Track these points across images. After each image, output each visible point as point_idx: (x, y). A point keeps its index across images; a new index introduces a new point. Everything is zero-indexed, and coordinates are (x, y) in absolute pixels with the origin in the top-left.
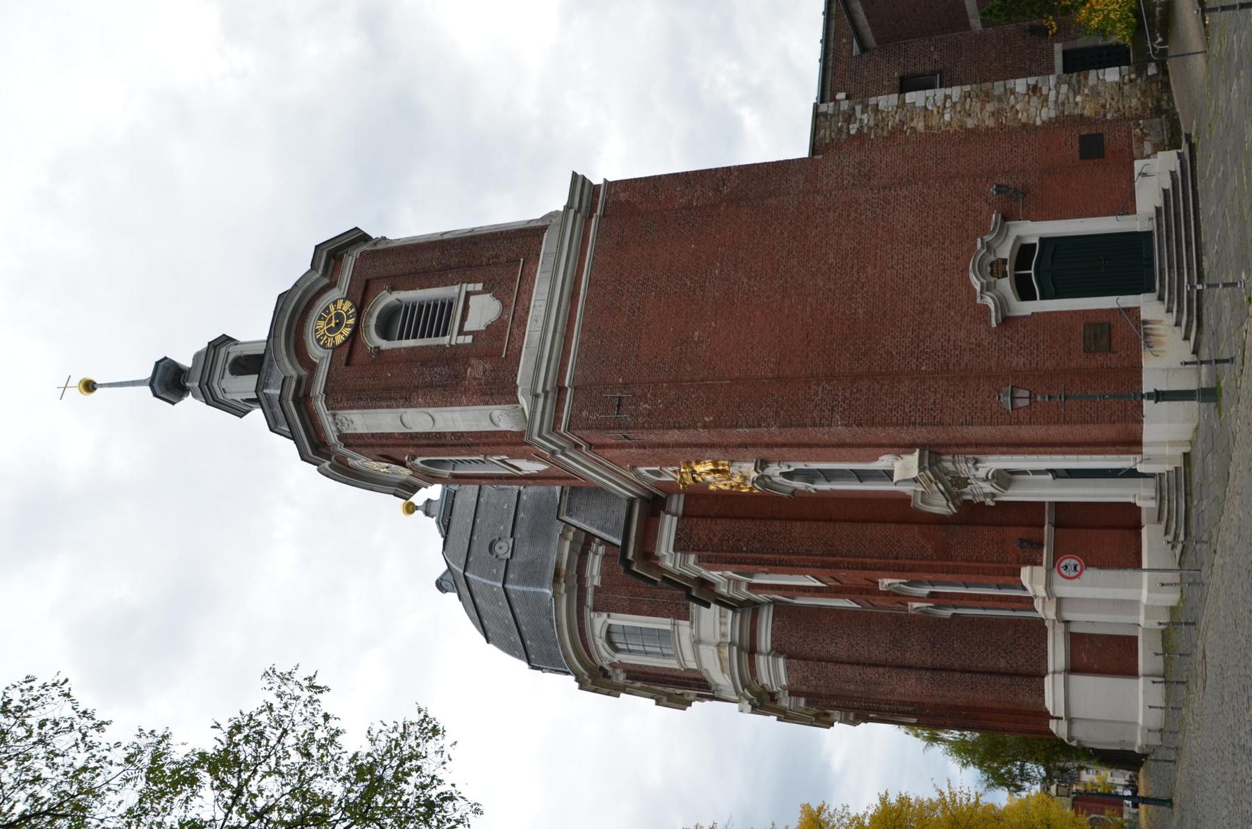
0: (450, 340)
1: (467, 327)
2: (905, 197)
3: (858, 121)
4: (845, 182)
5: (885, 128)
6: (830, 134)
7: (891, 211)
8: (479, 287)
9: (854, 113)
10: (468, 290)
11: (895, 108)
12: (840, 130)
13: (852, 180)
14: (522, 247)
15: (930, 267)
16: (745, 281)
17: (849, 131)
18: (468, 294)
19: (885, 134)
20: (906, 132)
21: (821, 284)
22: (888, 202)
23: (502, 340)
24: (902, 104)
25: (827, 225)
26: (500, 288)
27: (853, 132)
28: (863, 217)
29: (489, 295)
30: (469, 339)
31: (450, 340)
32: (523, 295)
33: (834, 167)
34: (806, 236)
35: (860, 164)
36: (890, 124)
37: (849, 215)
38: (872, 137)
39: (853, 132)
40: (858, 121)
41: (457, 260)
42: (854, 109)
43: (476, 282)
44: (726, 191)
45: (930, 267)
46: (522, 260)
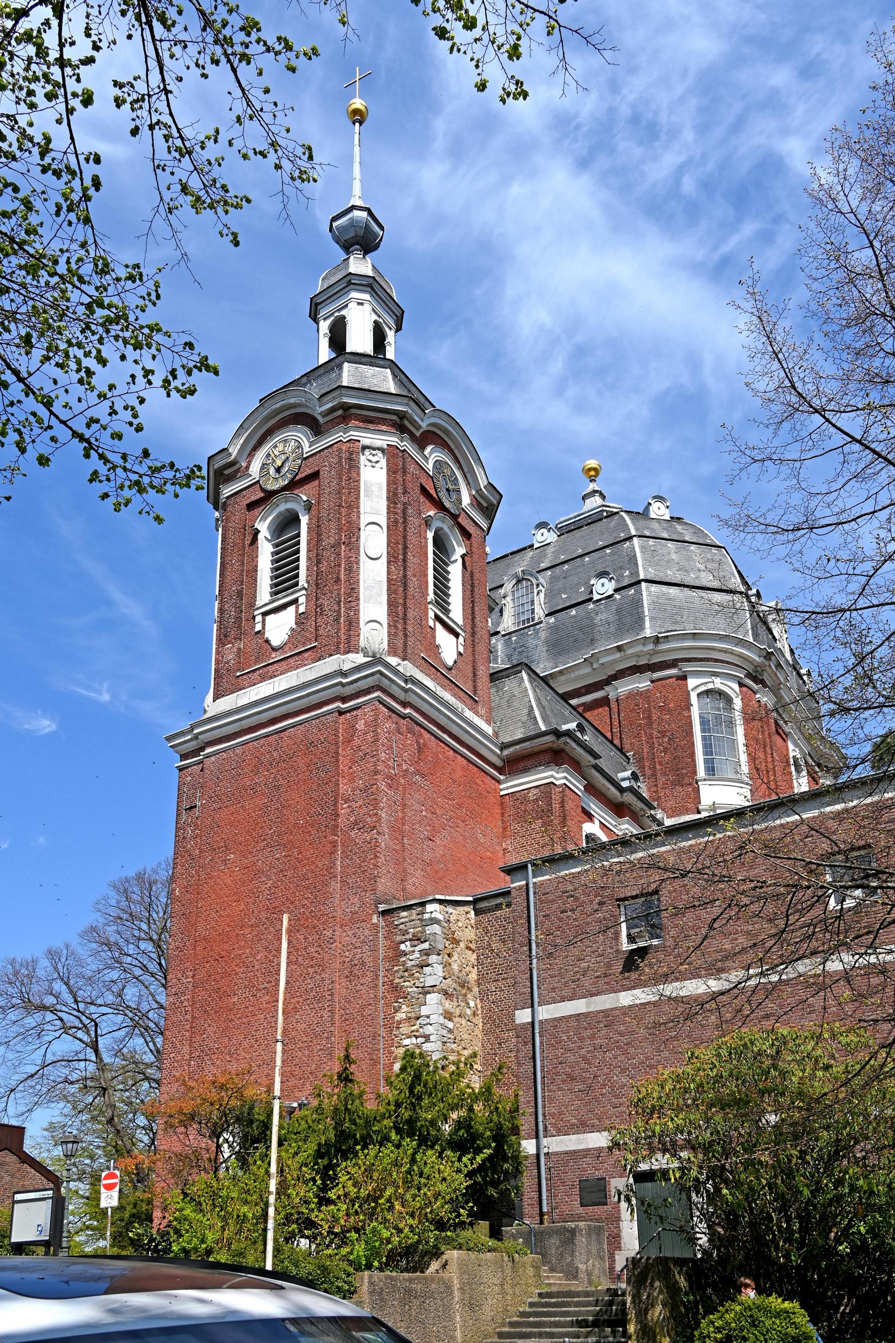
2: (322, 1017)
3: (412, 949)
4: (347, 954)
5: (402, 980)
6: (402, 923)
7: (312, 1006)
9: (422, 942)
11: (422, 985)
12: (406, 932)
13: (348, 959)
15: (262, 1053)
16: (267, 886)
17: (403, 942)
19: (397, 981)
20: (396, 1002)
21: (258, 958)
22: (319, 1001)
24: (425, 991)
25: (306, 948)
27: (402, 947)
28: (309, 981)
33: (363, 938)
34: (298, 931)
35: (363, 964)
36: (406, 984)
37: (312, 966)
38: (395, 968)
39: (403, 947)
40: (412, 949)
42: (425, 941)
44: (352, 834)
45: (262, 1053)
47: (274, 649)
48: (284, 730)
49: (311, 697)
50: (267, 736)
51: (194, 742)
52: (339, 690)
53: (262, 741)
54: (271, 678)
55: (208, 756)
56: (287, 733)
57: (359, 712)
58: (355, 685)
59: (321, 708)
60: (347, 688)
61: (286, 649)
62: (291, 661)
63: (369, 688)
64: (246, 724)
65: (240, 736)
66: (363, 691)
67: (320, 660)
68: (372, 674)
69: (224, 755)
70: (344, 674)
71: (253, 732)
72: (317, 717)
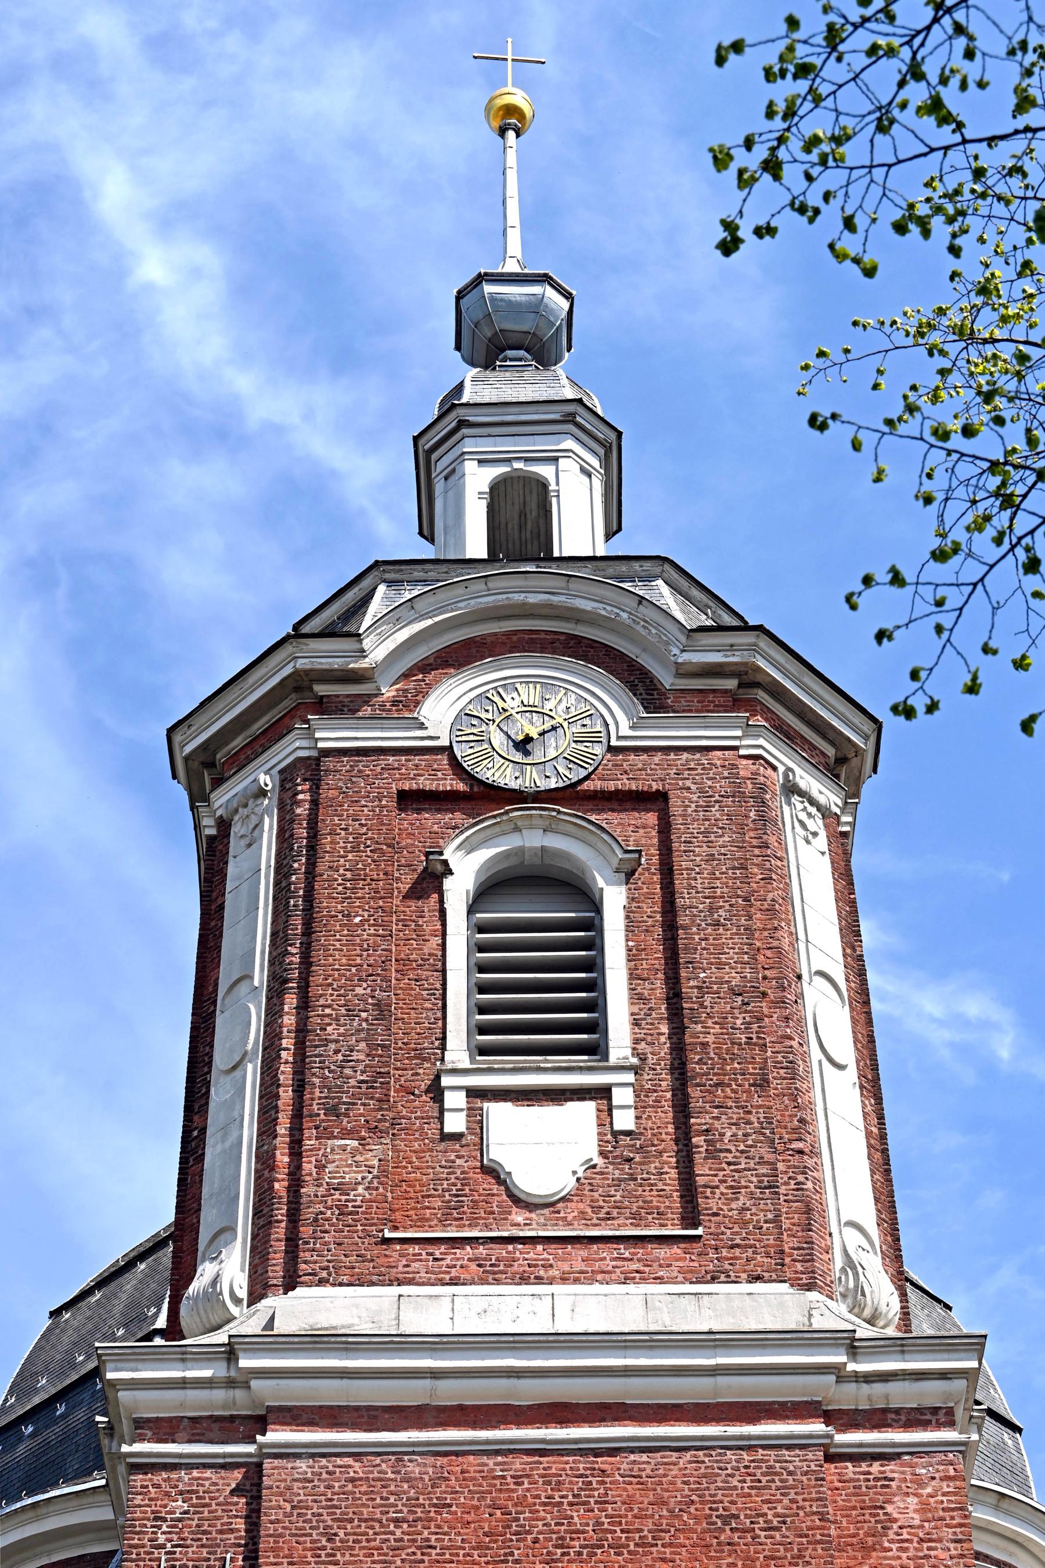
0: (455, 1071)
1: (497, 1112)
8: (624, 1120)
10: (615, 1091)
14: (745, 1223)
18: (603, 1093)
23: (443, 1223)
26: (618, 1183)
29: (592, 1152)
30: (455, 1123)
31: (455, 1071)
32: (584, 1253)
41: (710, 1039)
43: (640, 1106)
46: (699, 1231)
47: (518, 1201)
48: (613, 1452)
49: (722, 1381)
50: (542, 1453)
51: (219, 1395)
52: (823, 1387)
53: (518, 1464)
54: (524, 1280)
55: (287, 1453)
56: (624, 1462)
57: (891, 1468)
58: (878, 1388)
59: (753, 1420)
60: (851, 1388)
61: (570, 1211)
62: (606, 1252)
63: (919, 1410)
64: (449, 1393)
65: (421, 1426)
66: (897, 1411)
67: (713, 1280)
68: (944, 1375)
69: (357, 1468)
70: (853, 1346)
71: (474, 1425)
72: (748, 1445)
